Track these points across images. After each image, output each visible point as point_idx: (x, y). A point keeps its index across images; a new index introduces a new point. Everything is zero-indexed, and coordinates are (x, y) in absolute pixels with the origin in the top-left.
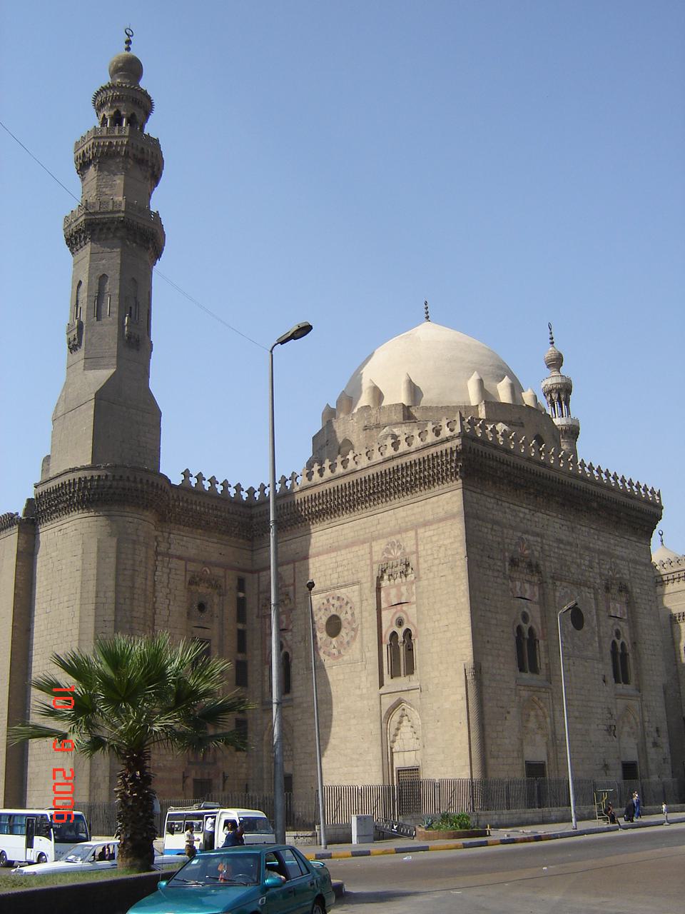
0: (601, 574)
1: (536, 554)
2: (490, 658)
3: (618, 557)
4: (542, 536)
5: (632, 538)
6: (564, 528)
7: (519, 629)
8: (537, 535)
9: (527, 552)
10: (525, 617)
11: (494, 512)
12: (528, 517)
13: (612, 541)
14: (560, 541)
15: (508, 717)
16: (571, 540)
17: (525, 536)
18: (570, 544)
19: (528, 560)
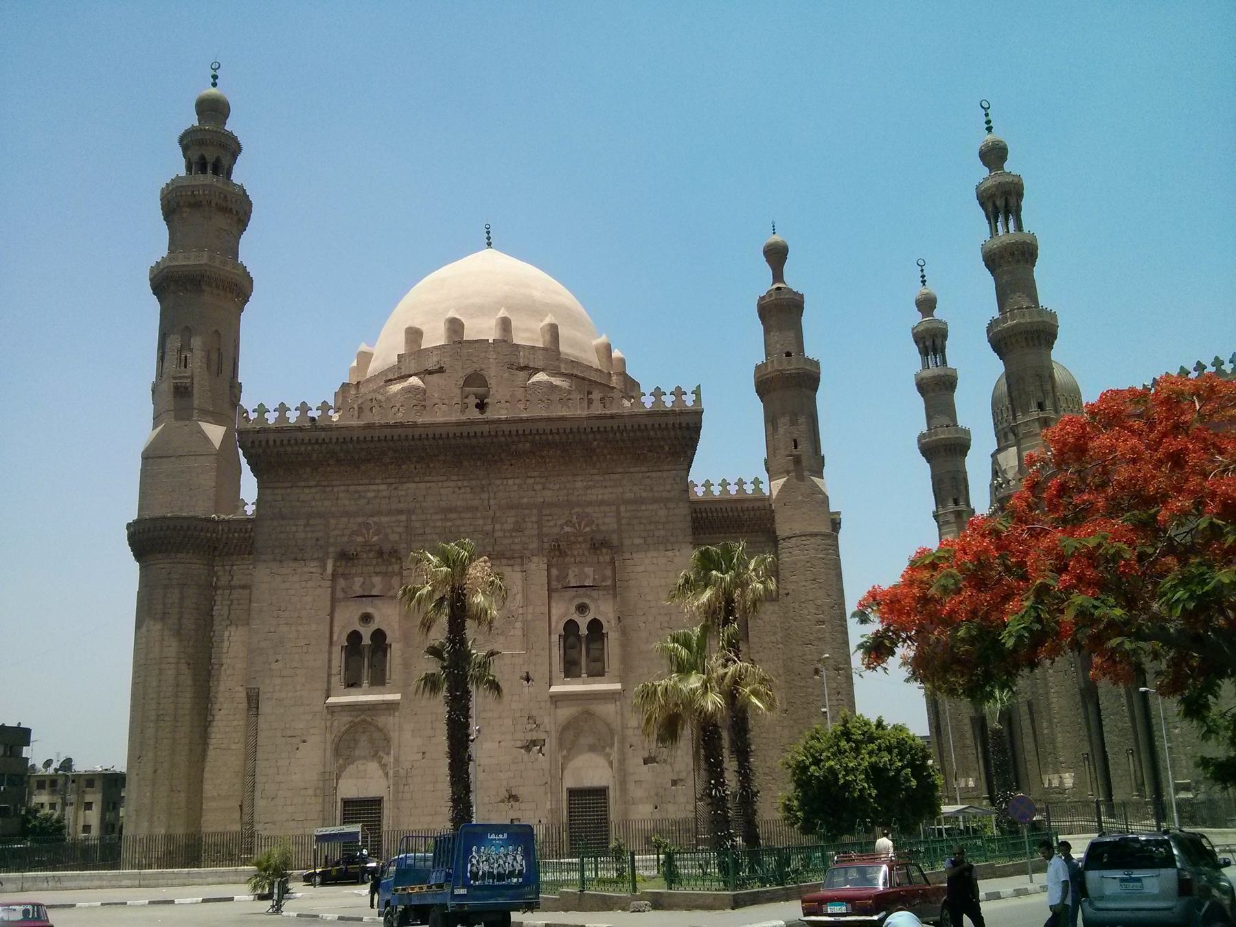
0: (540, 536)
1: (393, 537)
2: (278, 681)
3: (590, 504)
4: (410, 512)
5: (632, 470)
6: (463, 490)
7: (355, 637)
8: (401, 512)
9: (375, 538)
10: (366, 618)
11: (313, 503)
12: (384, 494)
13: (579, 485)
14: (452, 510)
15: (301, 746)
16: (476, 502)
17: (371, 520)
18: (469, 509)
19: (377, 548)
